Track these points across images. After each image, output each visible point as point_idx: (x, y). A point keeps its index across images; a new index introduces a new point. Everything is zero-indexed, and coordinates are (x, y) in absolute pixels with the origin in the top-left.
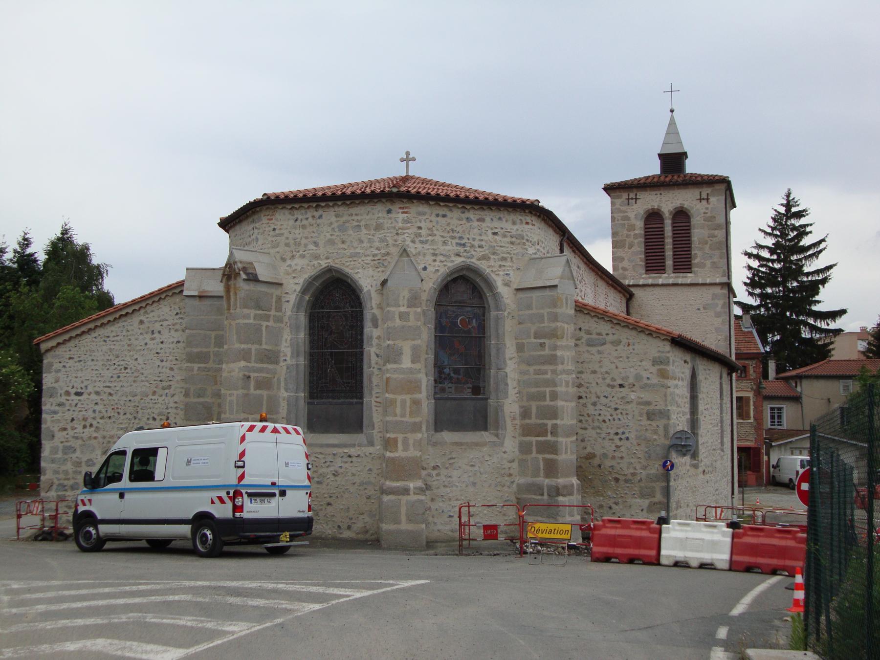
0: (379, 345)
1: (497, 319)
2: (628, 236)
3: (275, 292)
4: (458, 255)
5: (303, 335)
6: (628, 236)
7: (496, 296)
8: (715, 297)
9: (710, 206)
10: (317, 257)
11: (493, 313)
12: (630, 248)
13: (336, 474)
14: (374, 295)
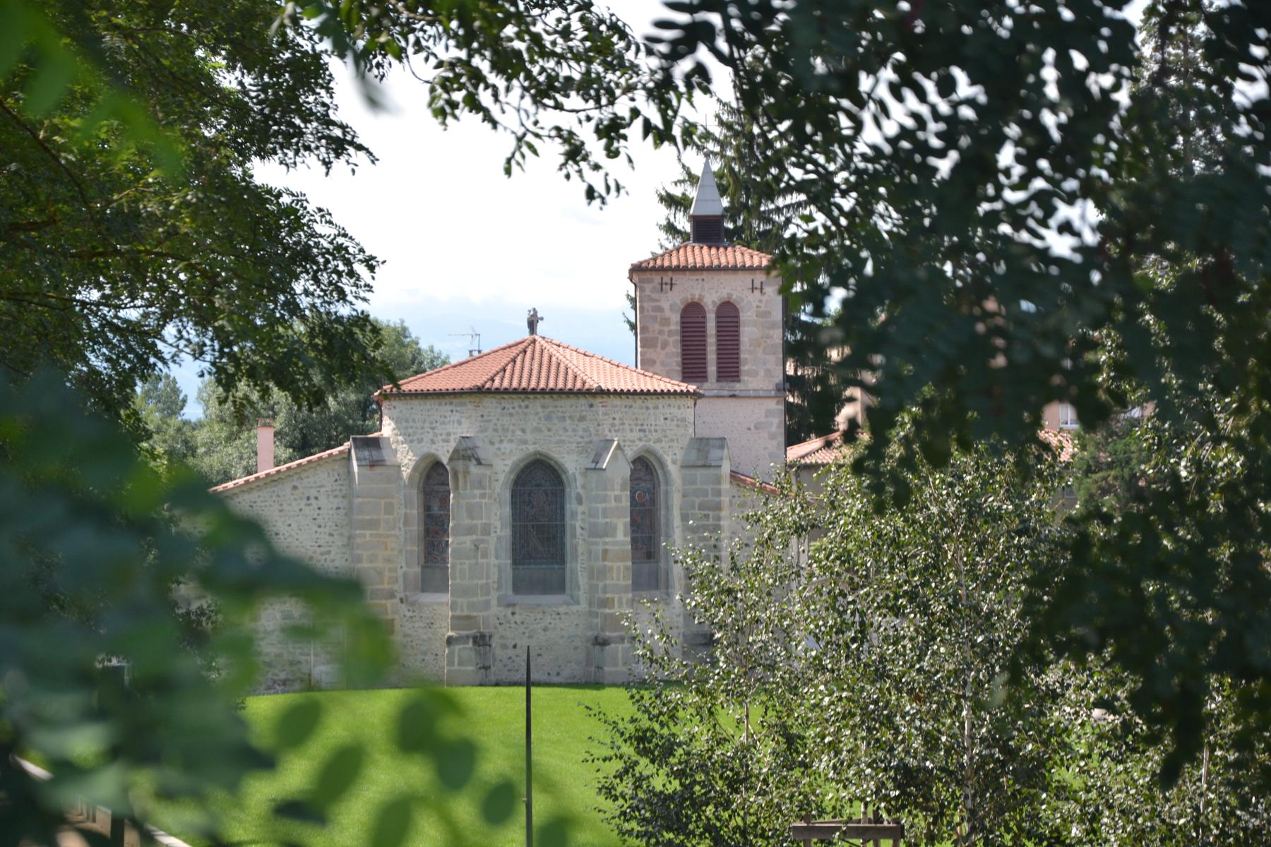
0: (583, 520)
1: (667, 493)
2: (661, 332)
3: (488, 472)
4: (640, 439)
5: (507, 510)
6: (661, 332)
7: (666, 473)
8: (769, 413)
9: (765, 298)
10: (525, 442)
11: (663, 487)
12: (663, 348)
13: (545, 629)
14: (578, 477)
